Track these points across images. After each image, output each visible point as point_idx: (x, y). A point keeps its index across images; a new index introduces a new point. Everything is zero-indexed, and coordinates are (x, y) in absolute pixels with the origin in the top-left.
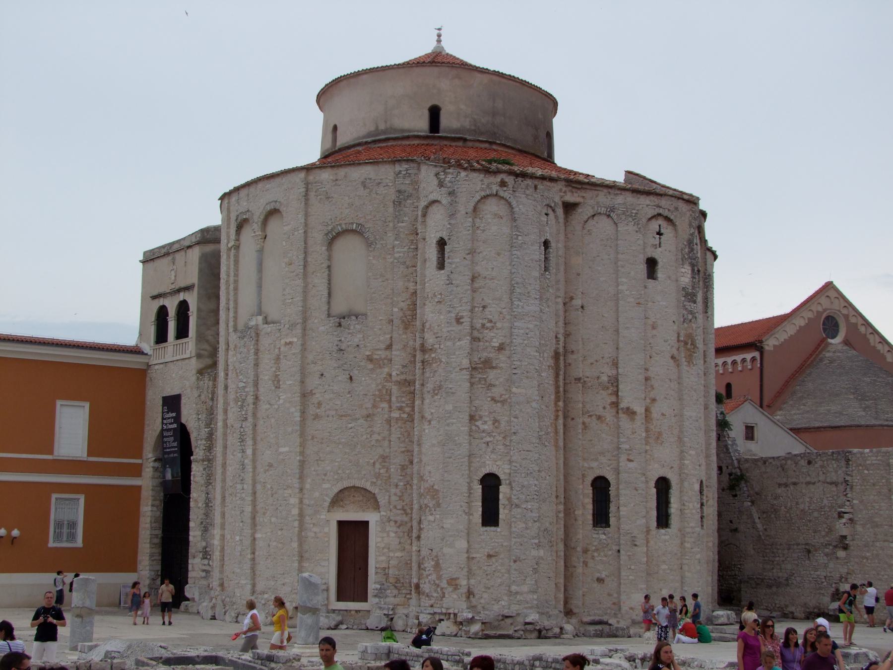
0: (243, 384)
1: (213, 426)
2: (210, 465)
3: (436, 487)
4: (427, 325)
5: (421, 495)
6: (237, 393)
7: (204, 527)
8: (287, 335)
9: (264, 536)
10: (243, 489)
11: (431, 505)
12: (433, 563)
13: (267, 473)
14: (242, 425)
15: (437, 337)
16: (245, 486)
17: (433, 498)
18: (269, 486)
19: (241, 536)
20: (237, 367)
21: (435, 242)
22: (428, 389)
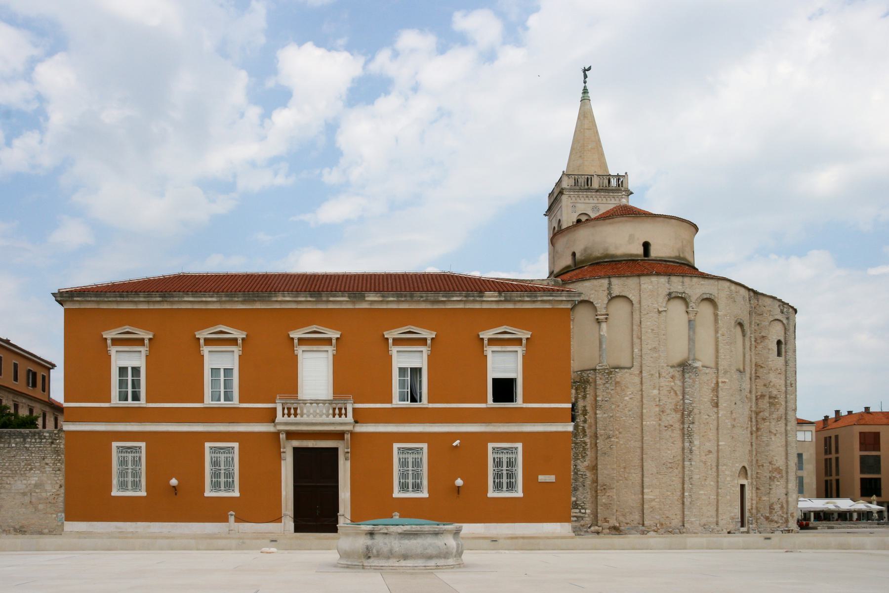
0: (691, 402)
1: (579, 421)
2: (576, 446)
3: (781, 468)
4: (772, 384)
5: (770, 472)
6: (677, 406)
7: (574, 488)
8: (723, 377)
9: (706, 492)
10: (691, 465)
11: (778, 477)
12: (780, 506)
13: (708, 456)
14: (689, 426)
15: (779, 392)
16: (693, 463)
17: (779, 473)
18: (709, 464)
19: (690, 492)
20: (676, 389)
21: (776, 341)
22: (774, 417)
